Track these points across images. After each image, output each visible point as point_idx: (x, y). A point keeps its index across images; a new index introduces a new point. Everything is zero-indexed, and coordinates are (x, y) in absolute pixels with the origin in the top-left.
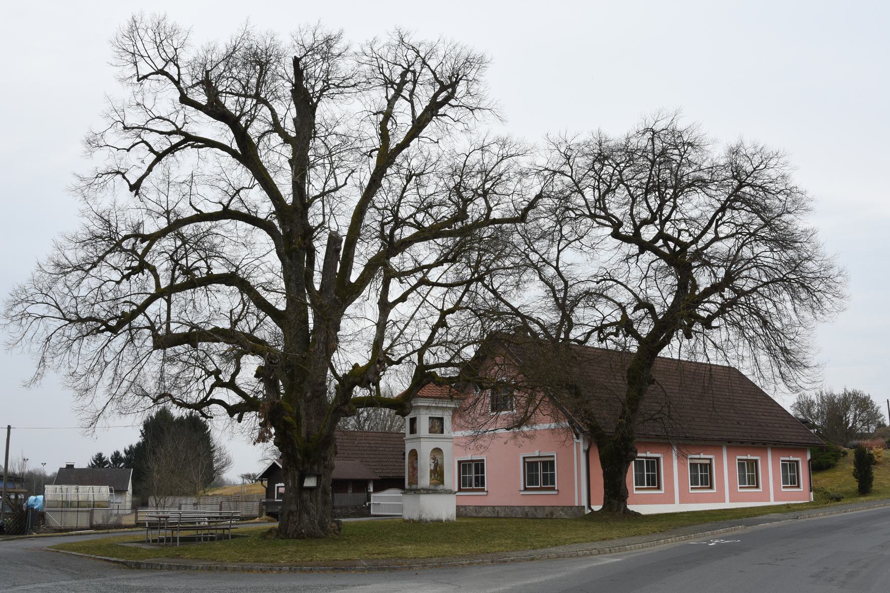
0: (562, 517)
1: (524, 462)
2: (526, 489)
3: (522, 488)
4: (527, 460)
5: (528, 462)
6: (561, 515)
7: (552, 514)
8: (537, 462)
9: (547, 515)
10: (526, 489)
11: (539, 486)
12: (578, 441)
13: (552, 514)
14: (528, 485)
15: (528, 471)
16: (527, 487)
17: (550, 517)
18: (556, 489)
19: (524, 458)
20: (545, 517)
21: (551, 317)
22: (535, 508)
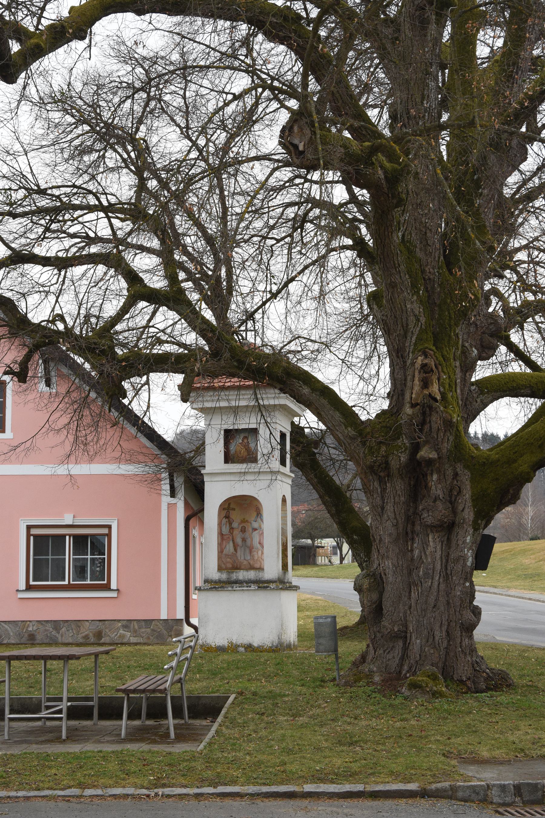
0: (125, 641)
1: (28, 535)
2: (29, 588)
3: (23, 586)
4: (34, 531)
5: (36, 537)
6: (122, 636)
7: (99, 635)
8: (64, 536)
9: (86, 637)
10: (29, 588)
11: (66, 582)
12: (173, 501)
13: (99, 635)
14: (34, 580)
15: (35, 555)
16: (32, 583)
17: (92, 640)
18: (114, 586)
19: (29, 528)
20: (81, 641)
21: (59, 368)
22: (56, 624)
